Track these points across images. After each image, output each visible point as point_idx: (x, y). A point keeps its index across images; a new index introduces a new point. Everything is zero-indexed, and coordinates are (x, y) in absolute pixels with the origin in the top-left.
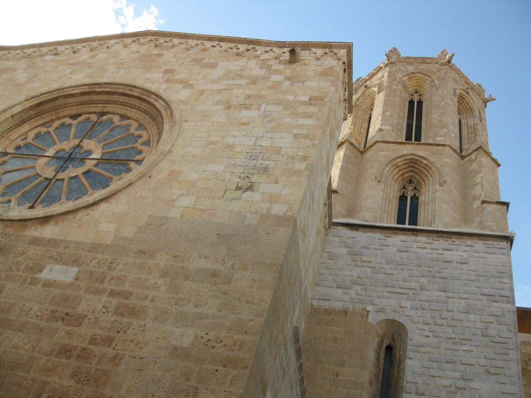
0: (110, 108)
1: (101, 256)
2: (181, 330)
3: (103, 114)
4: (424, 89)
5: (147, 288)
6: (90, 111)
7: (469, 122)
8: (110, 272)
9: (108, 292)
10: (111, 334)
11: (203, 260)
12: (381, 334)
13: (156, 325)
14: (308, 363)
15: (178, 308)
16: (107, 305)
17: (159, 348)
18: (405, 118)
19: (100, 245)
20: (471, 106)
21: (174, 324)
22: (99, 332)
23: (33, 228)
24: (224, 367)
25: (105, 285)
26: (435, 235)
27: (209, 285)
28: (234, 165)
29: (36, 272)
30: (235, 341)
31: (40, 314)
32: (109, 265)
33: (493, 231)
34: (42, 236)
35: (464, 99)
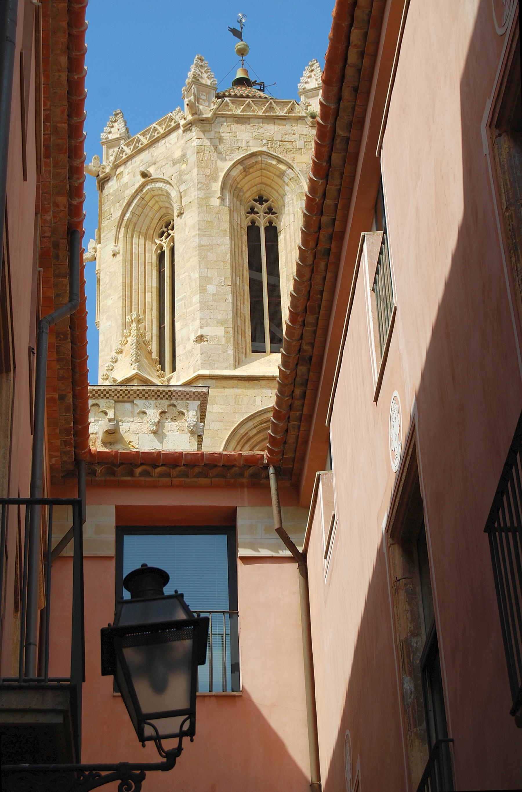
4: (277, 195)
18: (245, 285)
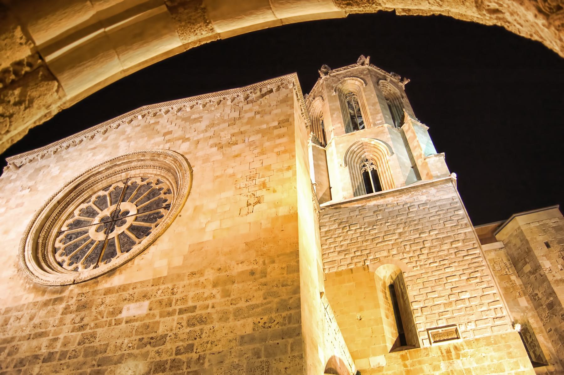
1: (162, 287)
2: (242, 322)
5: (206, 299)
8: (174, 296)
9: (178, 311)
10: (190, 342)
11: (240, 265)
13: (222, 325)
15: (234, 307)
16: (180, 322)
17: (230, 341)
19: (160, 278)
21: (235, 319)
22: (181, 343)
23: (104, 281)
25: (173, 307)
27: (251, 282)
28: (240, 188)
29: (117, 315)
30: (284, 318)
31: (130, 345)
32: (172, 291)
34: (113, 285)
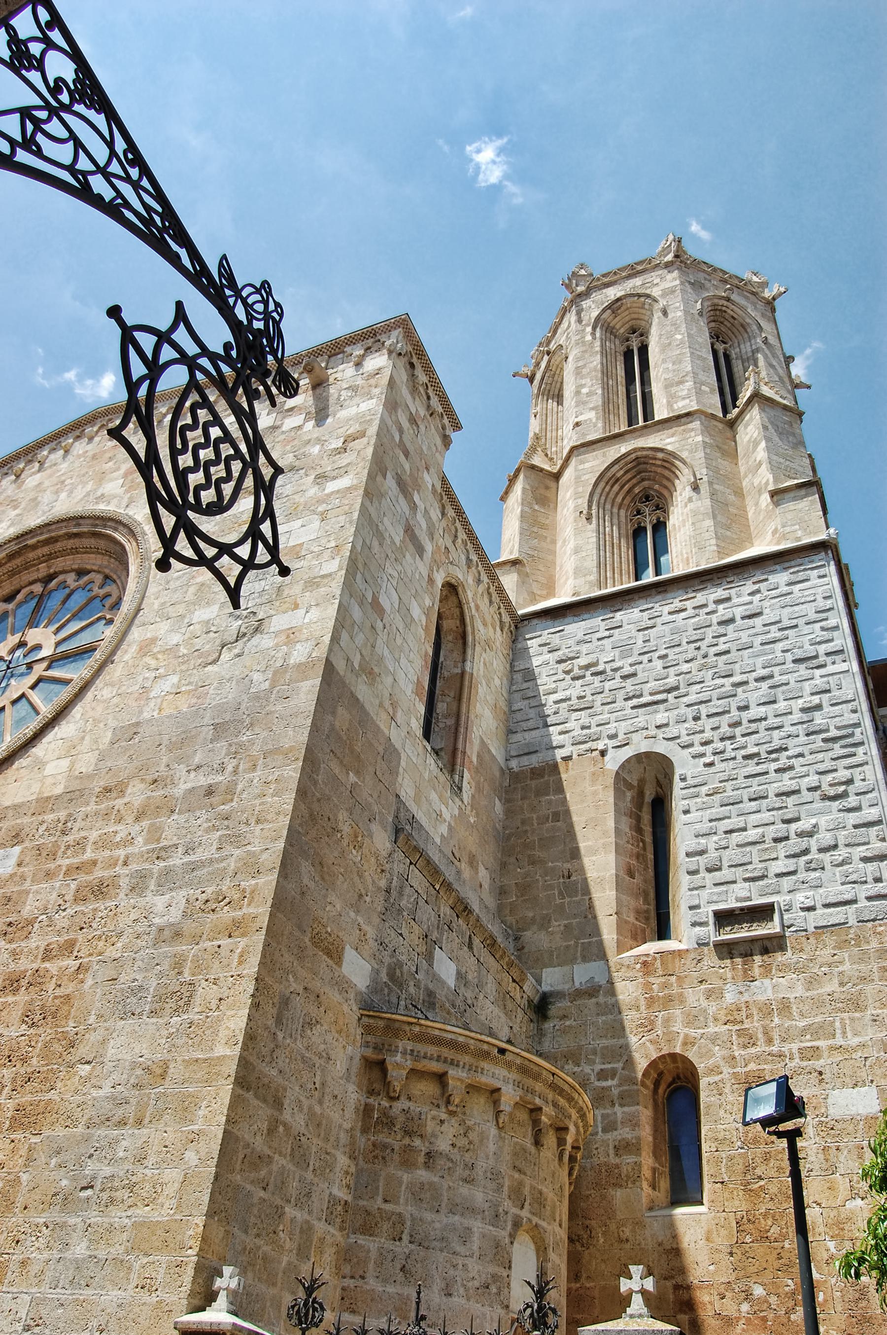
0: (59, 564)
3: (50, 578)
6: (31, 579)
7: (743, 351)
12: (635, 783)
14: (519, 870)
15: (162, 864)
20: (741, 321)
24: (230, 936)
26: (697, 581)
30: (244, 891)
33: (798, 539)
35: (725, 312)
